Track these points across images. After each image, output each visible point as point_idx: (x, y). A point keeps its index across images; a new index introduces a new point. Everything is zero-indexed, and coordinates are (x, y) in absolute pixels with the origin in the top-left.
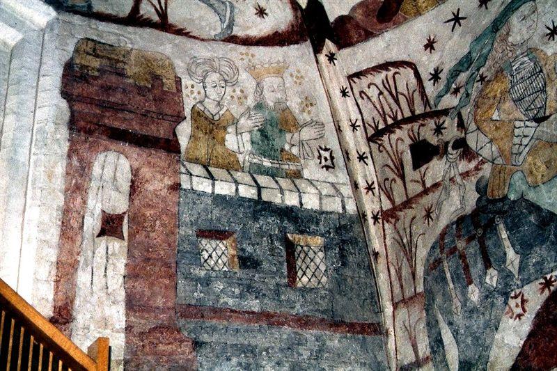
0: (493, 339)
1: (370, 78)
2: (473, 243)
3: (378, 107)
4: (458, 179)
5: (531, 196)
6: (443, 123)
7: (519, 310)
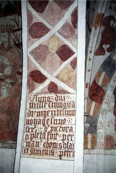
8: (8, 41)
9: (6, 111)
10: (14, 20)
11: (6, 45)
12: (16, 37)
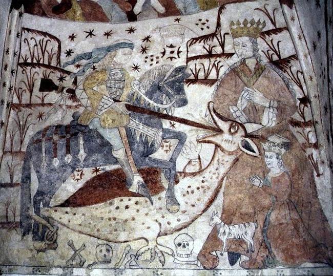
0: (60, 185)
1: (34, 35)
2: (63, 140)
3: (32, 51)
4: (64, 107)
5: (101, 131)
6: (66, 77)
7: (79, 177)
8: (254, 55)
9: (285, 202)
10: (264, 12)
11: (251, 63)
12: (273, 48)
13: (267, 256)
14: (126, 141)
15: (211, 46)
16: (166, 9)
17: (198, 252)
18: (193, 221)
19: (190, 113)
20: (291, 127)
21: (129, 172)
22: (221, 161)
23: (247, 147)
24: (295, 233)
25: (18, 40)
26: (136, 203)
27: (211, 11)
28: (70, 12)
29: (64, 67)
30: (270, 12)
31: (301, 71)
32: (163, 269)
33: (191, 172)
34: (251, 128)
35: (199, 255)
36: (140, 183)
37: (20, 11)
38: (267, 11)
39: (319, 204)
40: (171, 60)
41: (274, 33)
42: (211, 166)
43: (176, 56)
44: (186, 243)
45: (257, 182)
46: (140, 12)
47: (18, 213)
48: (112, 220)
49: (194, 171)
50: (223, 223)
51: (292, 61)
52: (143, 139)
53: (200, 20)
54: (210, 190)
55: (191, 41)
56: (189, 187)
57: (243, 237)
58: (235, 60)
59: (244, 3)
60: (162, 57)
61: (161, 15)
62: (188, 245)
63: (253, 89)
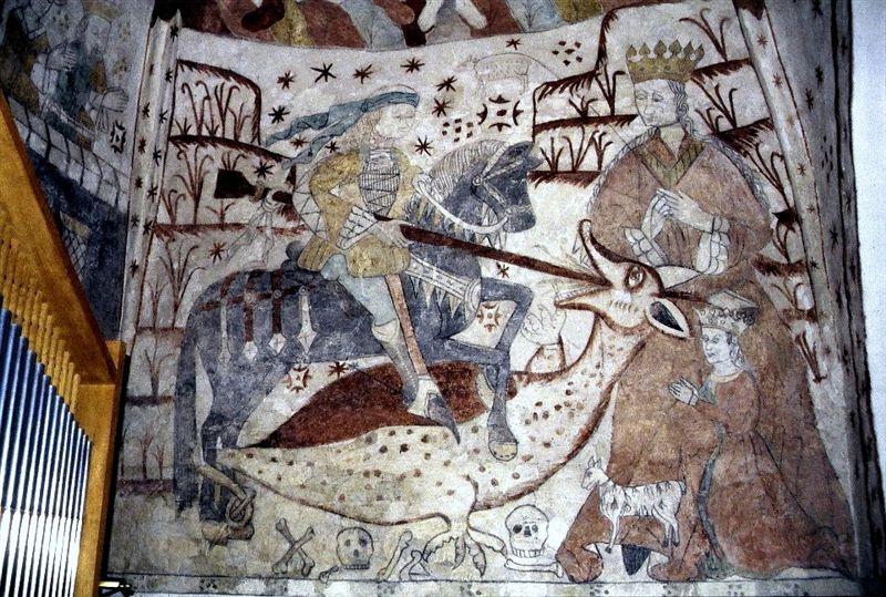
0: (260, 401)
1: (203, 76)
2: (266, 302)
3: (198, 110)
4: (268, 232)
5: (348, 283)
9: (746, 437)
10: (699, 25)
11: (673, 137)
12: (718, 102)
13: (707, 555)
14: (401, 306)
15: (586, 100)
16: (488, 19)
17: (559, 545)
18: (546, 478)
19: (540, 244)
20: (758, 274)
21: (409, 373)
22: (607, 349)
23: (664, 317)
24: (768, 504)
25: (169, 86)
26: (425, 439)
27: (585, 23)
28: (281, 27)
29: (267, 144)
30: (714, 26)
31: (780, 153)
32: (482, 582)
33: (542, 371)
34: (672, 276)
35: (560, 552)
36: (433, 397)
37: (172, 23)
38: (707, 24)
39: (820, 441)
40: (500, 130)
41: (722, 72)
42: (586, 359)
43: (511, 121)
44: (531, 526)
45: (685, 394)
46: (433, 27)
47: (168, 461)
48: (372, 475)
49: (549, 371)
50: (611, 483)
51: (761, 131)
52: (440, 301)
53: (563, 43)
54: (583, 411)
55: (542, 89)
56: (539, 404)
57: (655, 513)
58: (637, 129)
59: (658, 7)
60: (480, 124)
61: (477, 33)
62: (536, 529)
63: (676, 192)
